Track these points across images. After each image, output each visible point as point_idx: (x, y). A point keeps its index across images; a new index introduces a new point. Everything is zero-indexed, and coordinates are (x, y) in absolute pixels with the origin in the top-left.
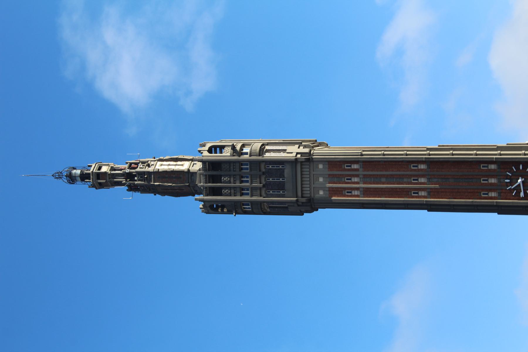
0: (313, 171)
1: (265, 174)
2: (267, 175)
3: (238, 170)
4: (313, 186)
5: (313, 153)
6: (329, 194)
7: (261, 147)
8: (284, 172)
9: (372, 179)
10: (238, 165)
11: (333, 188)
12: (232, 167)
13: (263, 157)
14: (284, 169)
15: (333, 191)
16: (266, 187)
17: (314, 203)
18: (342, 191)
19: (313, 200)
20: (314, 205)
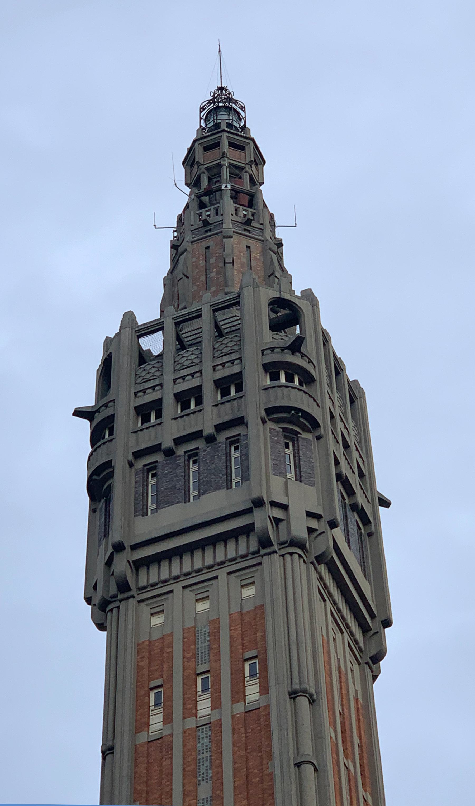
0: (229, 573)
1: (208, 447)
2: (205, 451)
3: (219, 375)
4: (177, 587)
5: (291, 554)
6: (150, 642)
7: (298, 410)
8: (218, 488)
9: (208, 754)
10: (236, 369)
11: (171, 646)
12: (226, 359)
13: (264, 422)
14: (229, 487)
15: (162, 650)
16: (165, 462)
17: (118, 607)
18: (162, 676)
19: (127, 599)
20: (111, 610)
